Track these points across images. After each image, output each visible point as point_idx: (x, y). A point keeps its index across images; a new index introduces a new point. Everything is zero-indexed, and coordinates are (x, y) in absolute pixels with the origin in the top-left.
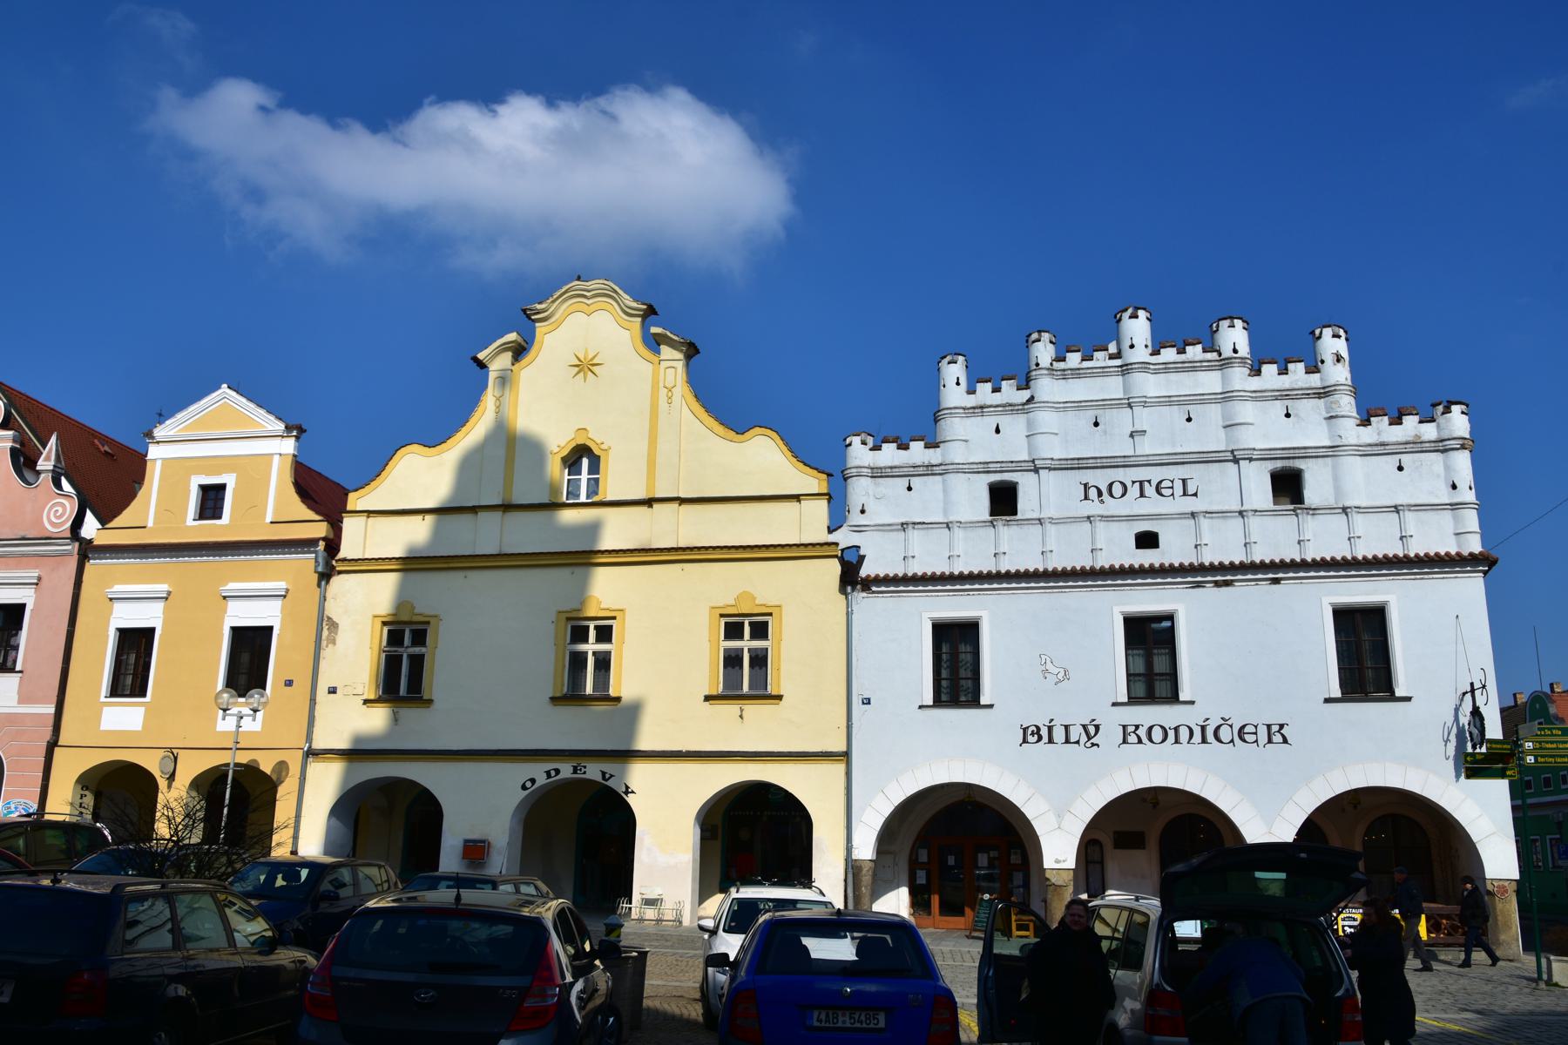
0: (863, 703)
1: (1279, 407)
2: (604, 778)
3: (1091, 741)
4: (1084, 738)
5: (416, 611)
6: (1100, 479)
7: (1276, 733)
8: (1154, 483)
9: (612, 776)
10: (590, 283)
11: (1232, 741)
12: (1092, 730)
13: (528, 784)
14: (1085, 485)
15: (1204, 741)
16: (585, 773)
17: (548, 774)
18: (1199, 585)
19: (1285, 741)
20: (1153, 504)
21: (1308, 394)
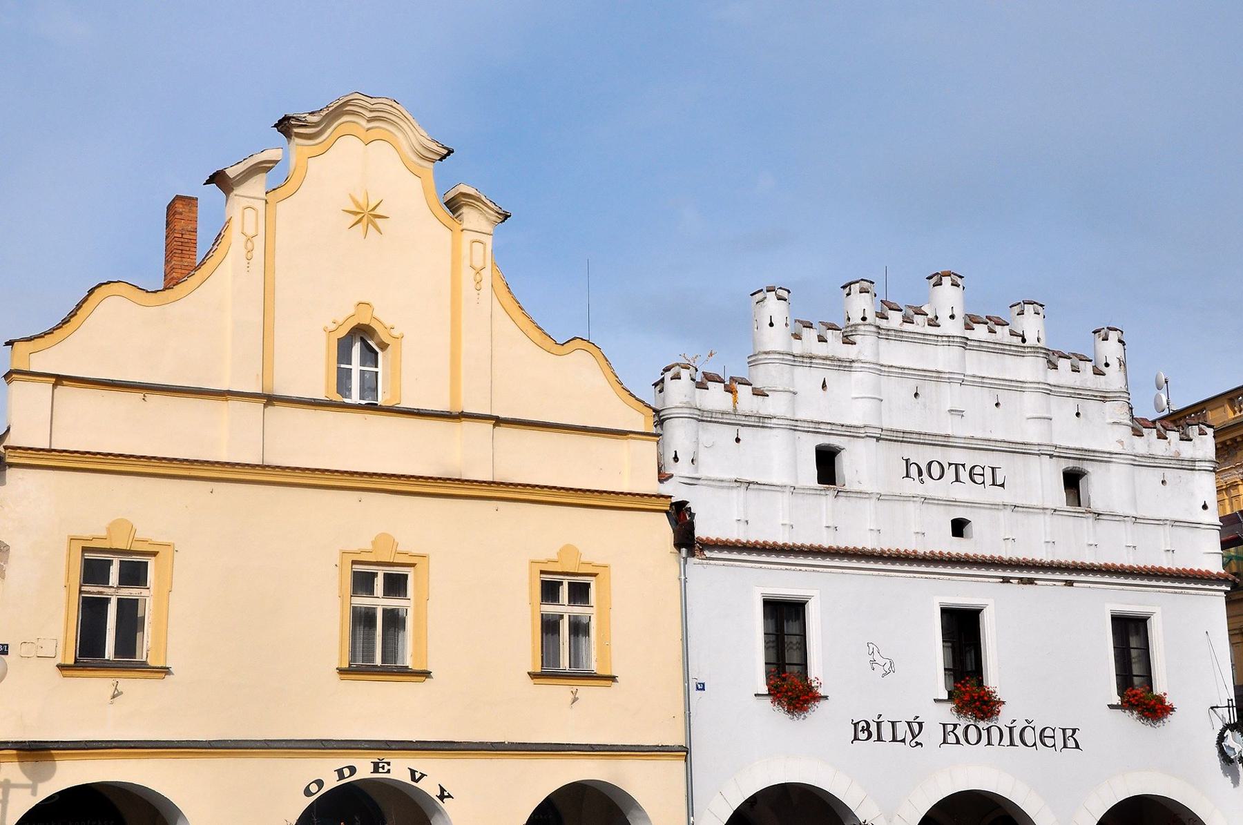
0: (698, 689)
1: (1071, 405)
2: (413, 779)
3: (915, 740)
4: (909, 737)
5: (138, 536)
6: (921, 456)
7: (1070, 738)
8: (968, 468)
9: (423, 775)
10: (374, 101)
11: (1035, 744)
12: (916, 727)
13: (314, 788)
14: (907, 461)
15: (1012, 744)
16: (389, 771)
17: (340, 772)
18: (1006, 580)
19: (1077, 747)
20: (965, 491)
21: (1096, 396)
